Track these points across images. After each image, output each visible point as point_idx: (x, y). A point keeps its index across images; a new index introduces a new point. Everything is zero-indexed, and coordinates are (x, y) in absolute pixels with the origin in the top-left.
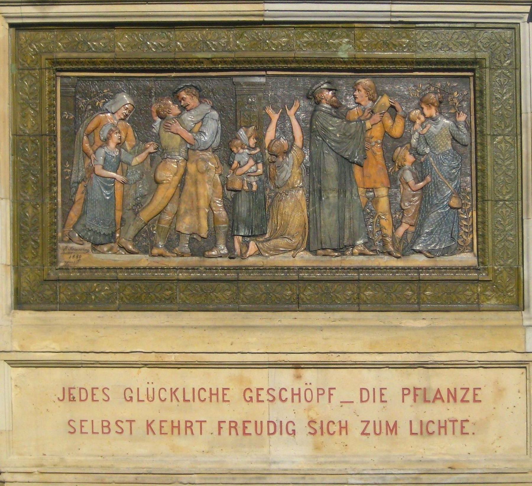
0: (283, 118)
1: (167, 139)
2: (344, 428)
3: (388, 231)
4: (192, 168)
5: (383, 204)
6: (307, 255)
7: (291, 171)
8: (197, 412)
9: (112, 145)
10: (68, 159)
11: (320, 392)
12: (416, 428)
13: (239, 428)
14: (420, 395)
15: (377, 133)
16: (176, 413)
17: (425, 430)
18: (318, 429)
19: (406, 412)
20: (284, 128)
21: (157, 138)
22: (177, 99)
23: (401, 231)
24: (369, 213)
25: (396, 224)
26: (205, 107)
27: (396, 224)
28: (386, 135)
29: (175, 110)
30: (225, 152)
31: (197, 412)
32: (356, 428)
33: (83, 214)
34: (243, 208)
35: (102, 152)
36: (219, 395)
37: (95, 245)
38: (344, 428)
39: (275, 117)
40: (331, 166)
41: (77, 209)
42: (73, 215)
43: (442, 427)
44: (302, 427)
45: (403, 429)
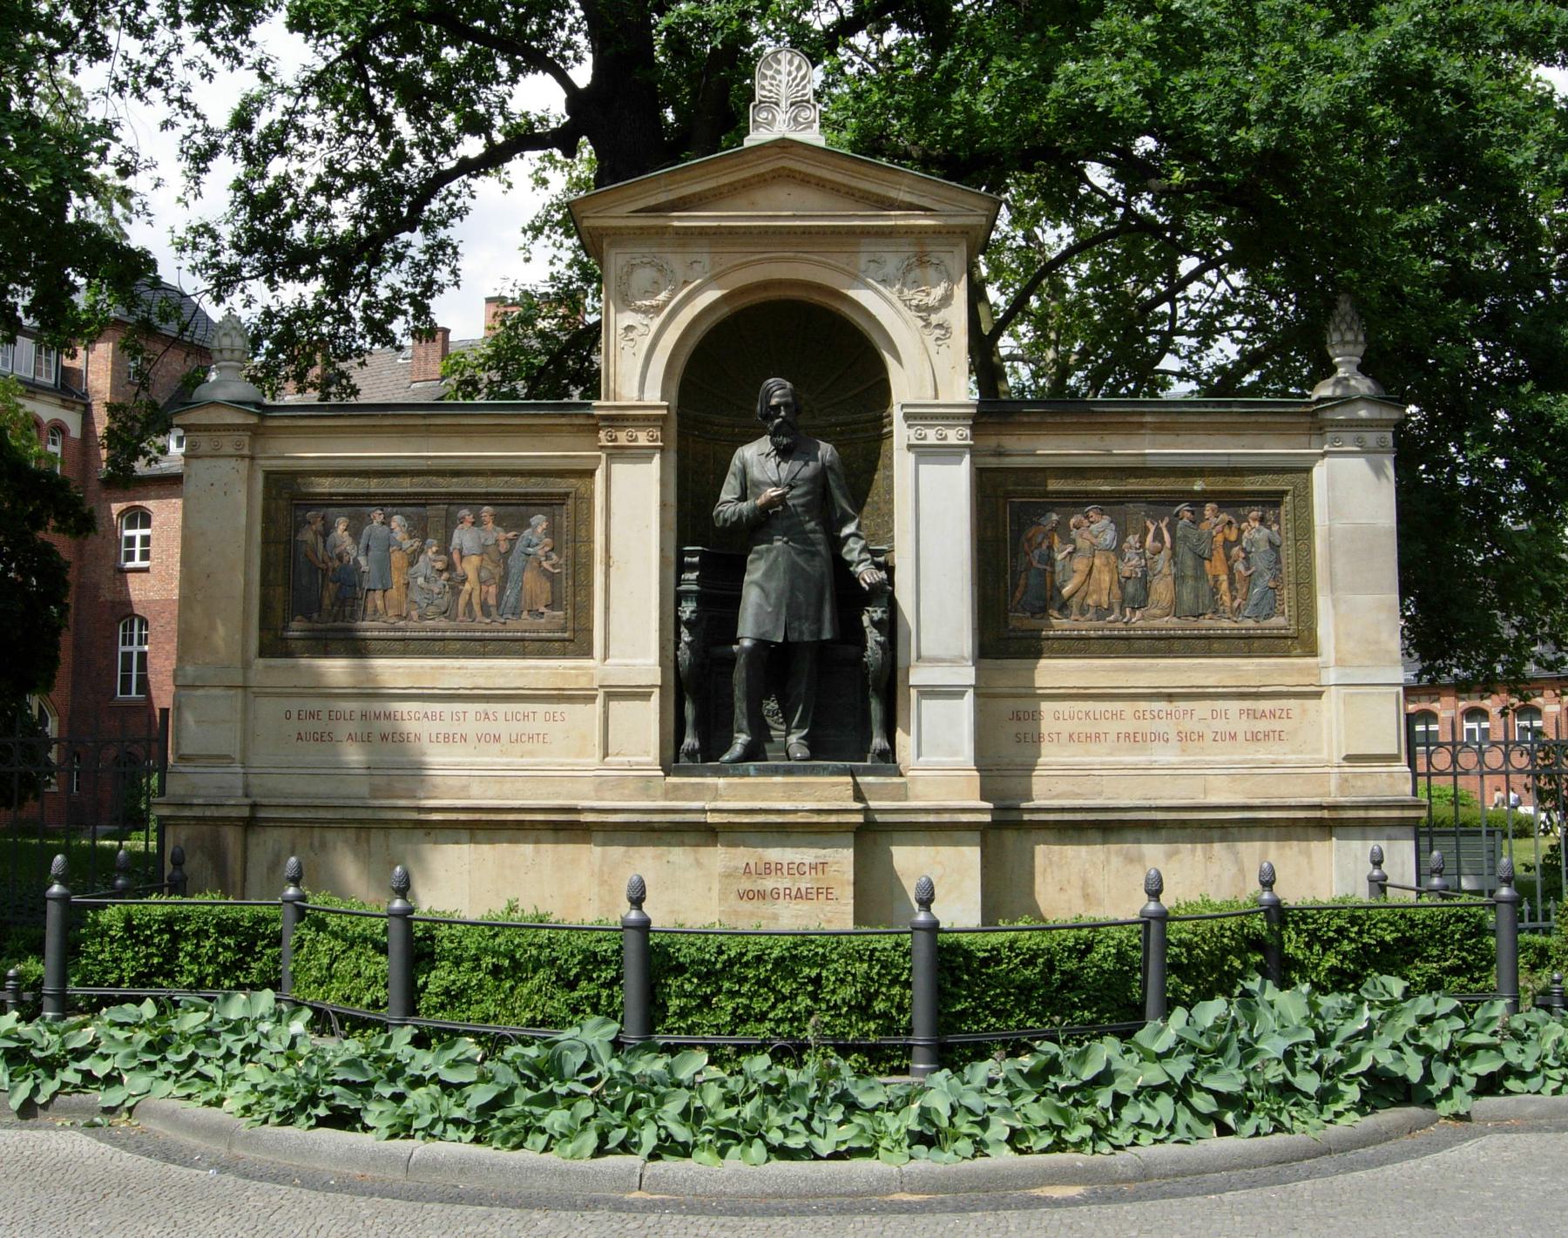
0: (1158, 530)
1: (1079, 542)
2: (1201, 737)
3: (1228, 603)
4: (1097, 562)
5: (1224, 586)
6: (1175, 620)
7: (1163, 563)
8: (1104, 726)
9: (1044, 546)
10: (1015, 555)
11: (1185, 712)
12: (1249, 736)
13: (1132, 738)
14: (1253, 715)
15: (1220, 538)
16: (1088, 727)
17: (1254, 737)
18: (1184, 737)
19: (1243, 726)
20: (1158, 536)
21: (1073, 542)
22: (1087, 517)
23: (1236, 604)
24: (1215, 591)
25: (1233, 599)
26: (1105, 520)
27: (1233, 599)
28: (1226, 540)
29: (1086, 522)
30: (1119, 552)
31: (1104, 726)
32: (1209, 736)
33: (1024, 593)
34: (1130, 588)
35: (1037, 552)
36: (1118, 716)
37: (1033, 614)
38: (1201, 737)
39: (1152, 528)
40: (1189, 561)
41: (1021, 588)
42: (1018, 594)
43: (1267, 736)
44: (1173, 736)
45: (1241, 737)
